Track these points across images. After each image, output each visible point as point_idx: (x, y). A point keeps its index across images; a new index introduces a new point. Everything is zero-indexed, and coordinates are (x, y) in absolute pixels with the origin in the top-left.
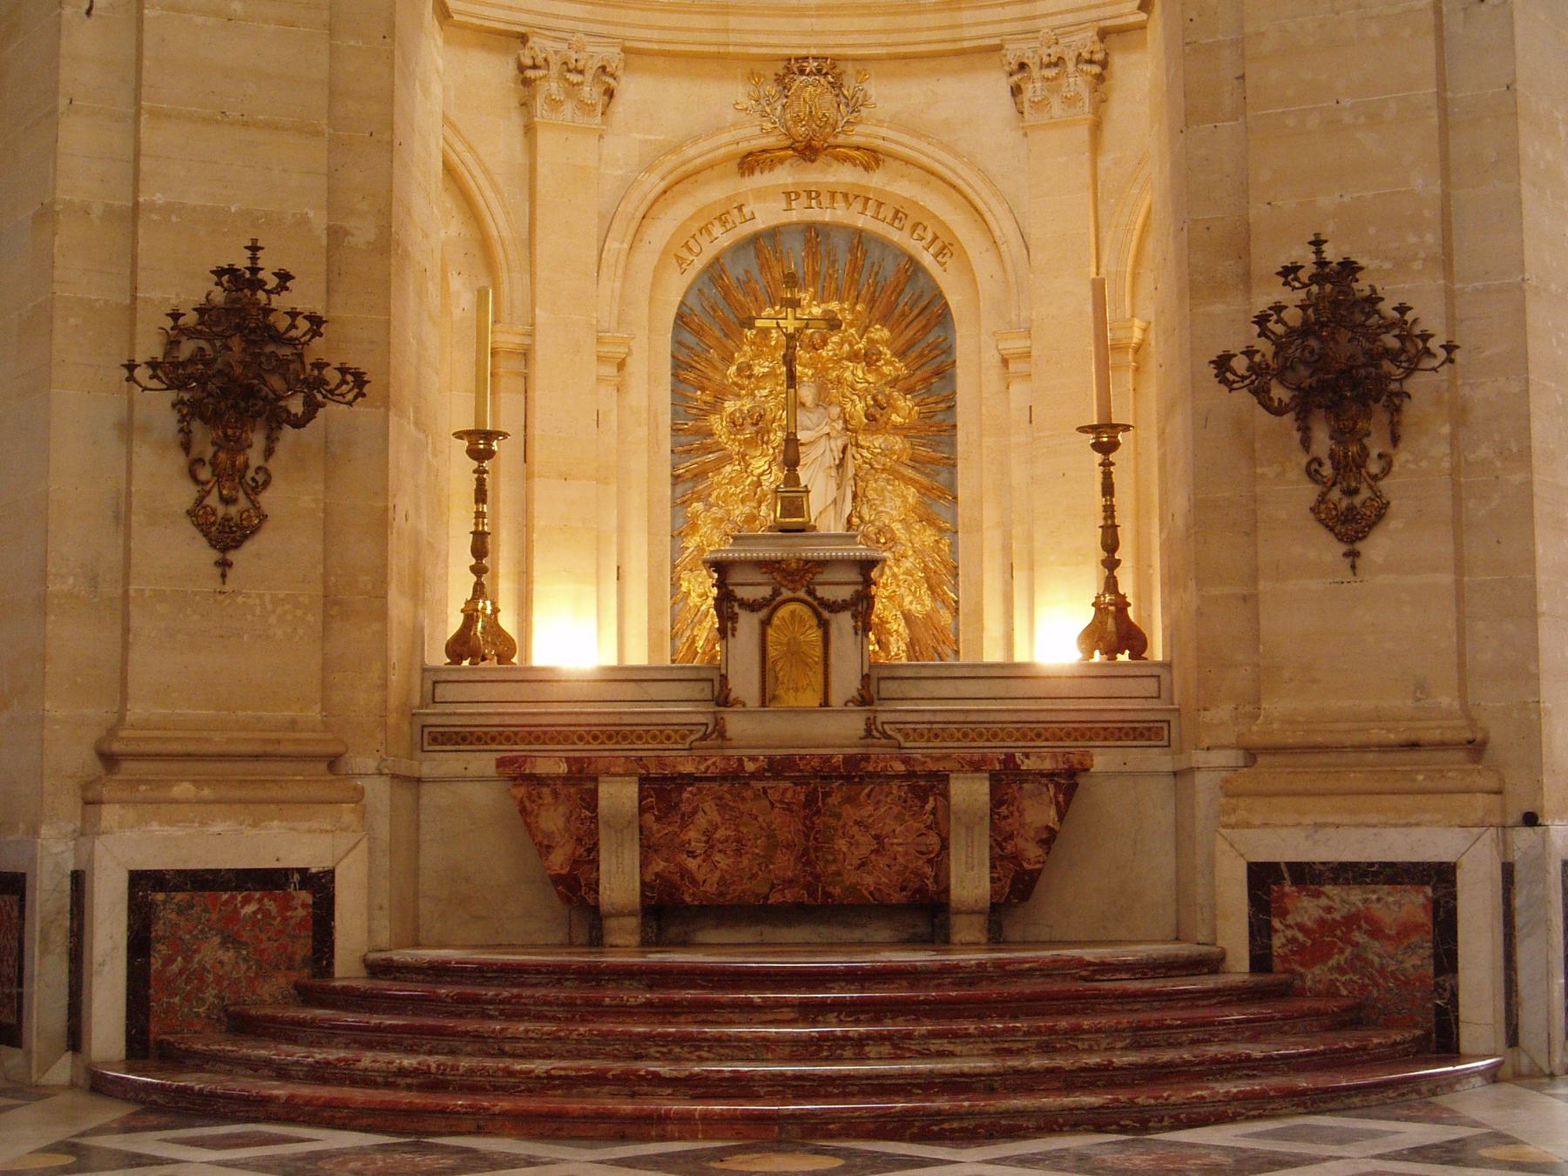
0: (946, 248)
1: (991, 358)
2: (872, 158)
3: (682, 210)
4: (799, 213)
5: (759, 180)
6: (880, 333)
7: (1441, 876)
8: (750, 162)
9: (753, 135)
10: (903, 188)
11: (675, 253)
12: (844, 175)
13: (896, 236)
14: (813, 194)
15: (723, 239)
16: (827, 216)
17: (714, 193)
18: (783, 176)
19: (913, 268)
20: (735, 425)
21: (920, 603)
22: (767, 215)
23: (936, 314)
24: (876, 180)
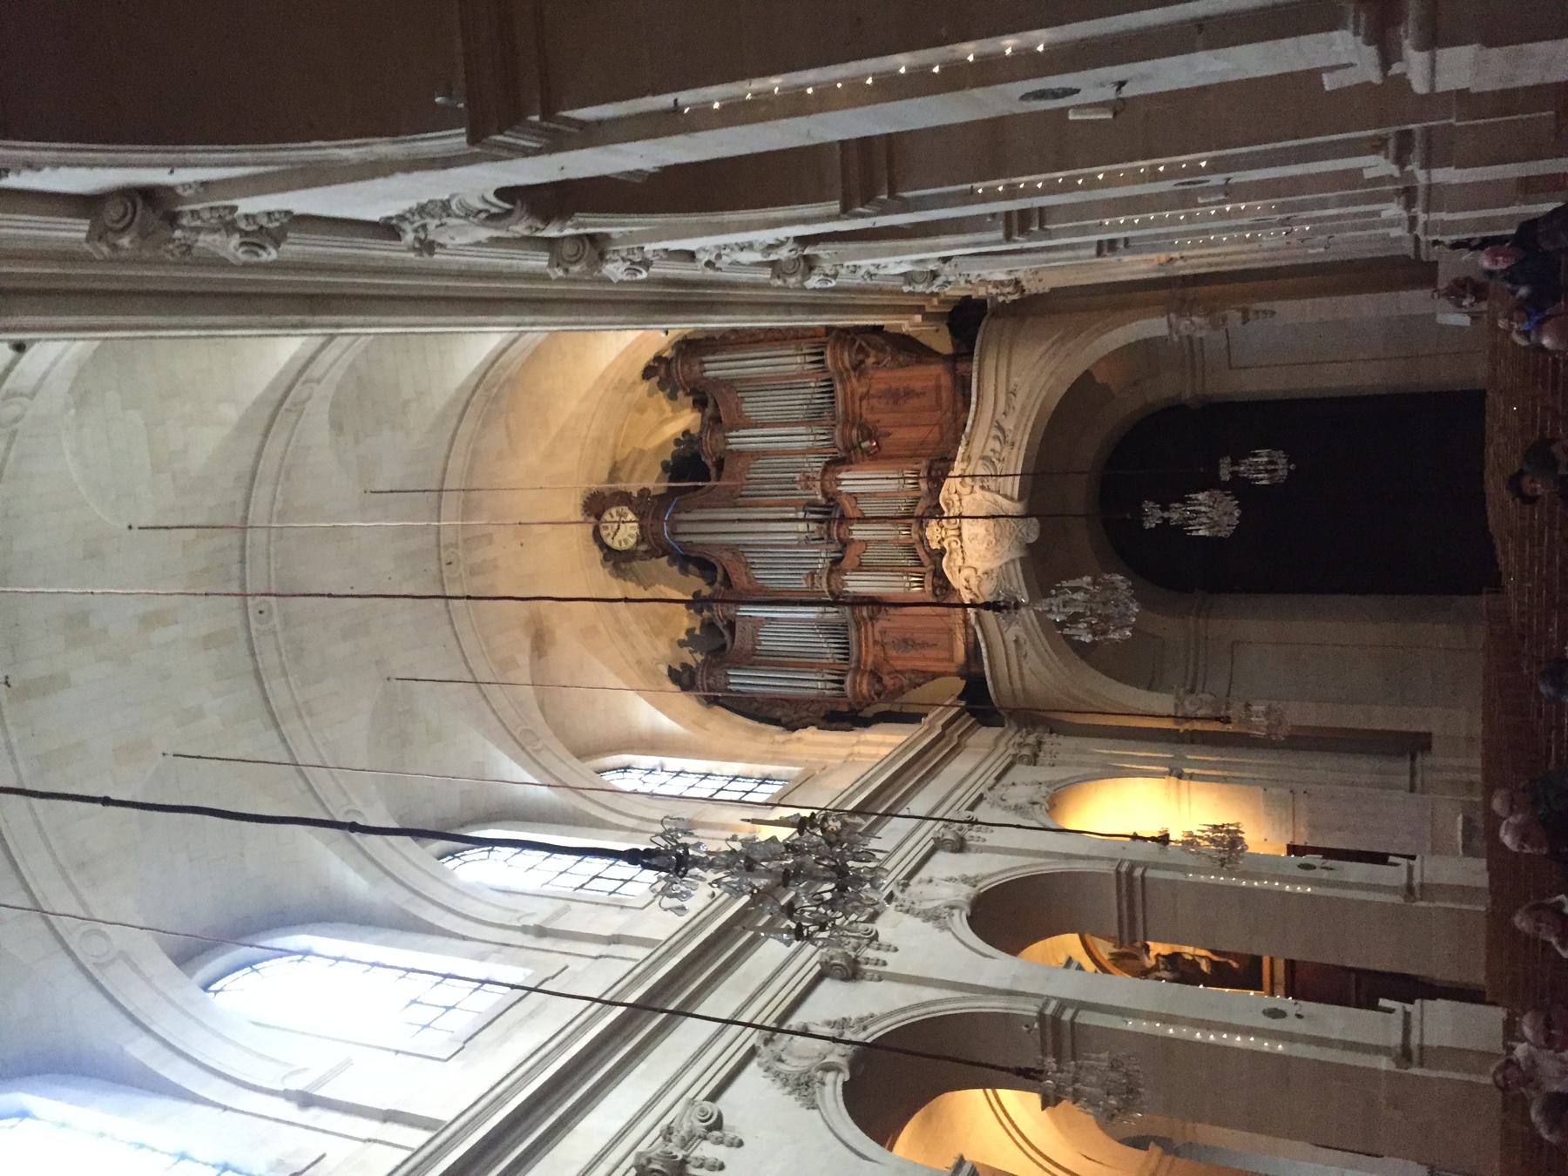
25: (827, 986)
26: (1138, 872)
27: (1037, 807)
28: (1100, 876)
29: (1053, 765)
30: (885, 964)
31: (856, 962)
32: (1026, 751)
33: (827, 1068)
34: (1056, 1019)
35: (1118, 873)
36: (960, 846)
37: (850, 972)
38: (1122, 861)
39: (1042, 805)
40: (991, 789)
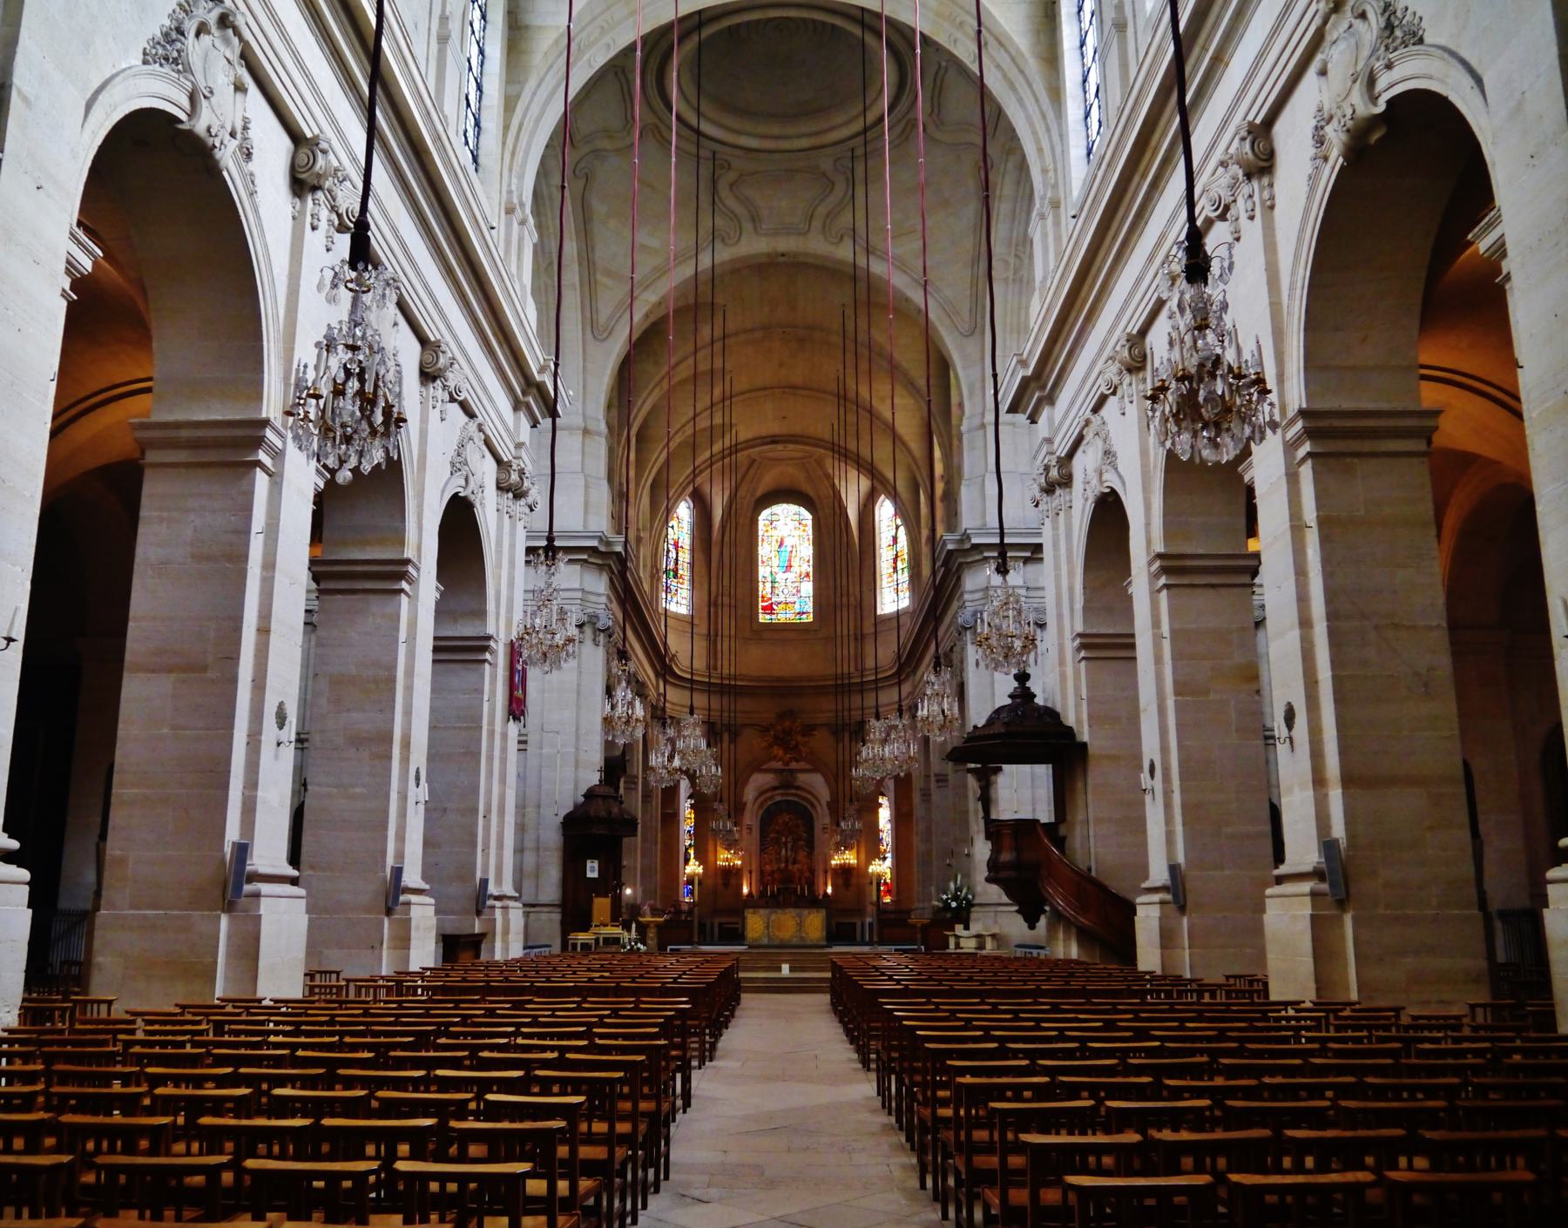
0: (813, 805)
1: (821, 827)
2: (798, 788)
3: (762, 798)
4: (784, 798)
5: (778, 792)
6: (800, 821)
7: (855, 924)
8: (775, 788)
9: (776, 783)
10: (804, 794)
11: (761, 806)
12: (793, 791)
13: (805, 804)
14: (787, 795)
15: (770, 803)
16: (789, 798)
17: (769, 794)
18: (781, 791)
19: (806, 808)
20: (772, 839)
21: (807, 874)
22: (778, 798)
23: (812, 818)
24: (799, 792)
25: (285, 143)
26: (404, 585)
27: (463, 483)
28: (401, 542)
29: (498, 510)
30: (314, 228)
31: (315, 188)
32: (514, 477)
33: (192, 98)
34: (258, 442)
35: (408, 562)
36: (428, 376)
37: (303, 176)
38: (418, 569)
39: (465, 488)
40: (480, 429)
